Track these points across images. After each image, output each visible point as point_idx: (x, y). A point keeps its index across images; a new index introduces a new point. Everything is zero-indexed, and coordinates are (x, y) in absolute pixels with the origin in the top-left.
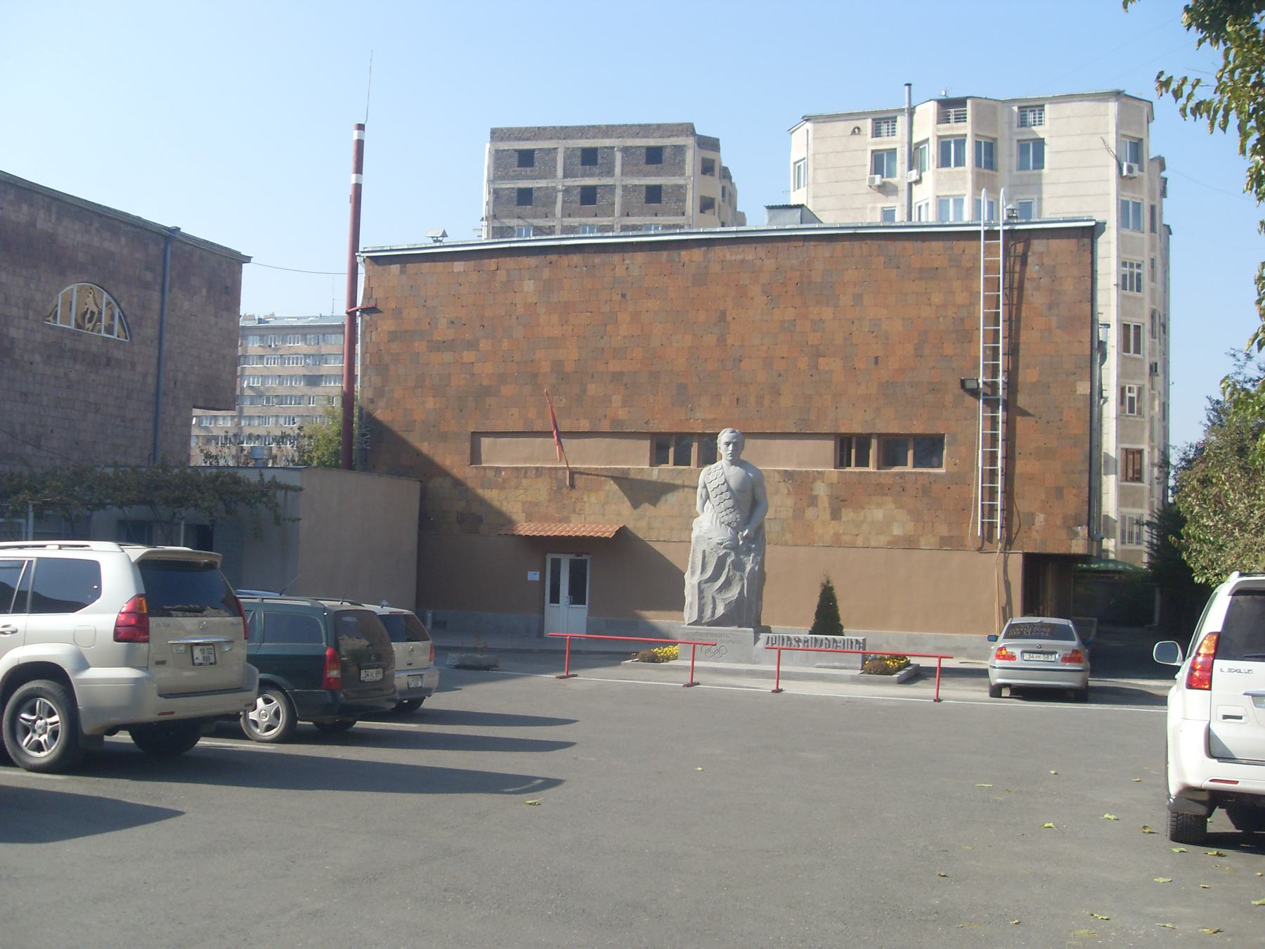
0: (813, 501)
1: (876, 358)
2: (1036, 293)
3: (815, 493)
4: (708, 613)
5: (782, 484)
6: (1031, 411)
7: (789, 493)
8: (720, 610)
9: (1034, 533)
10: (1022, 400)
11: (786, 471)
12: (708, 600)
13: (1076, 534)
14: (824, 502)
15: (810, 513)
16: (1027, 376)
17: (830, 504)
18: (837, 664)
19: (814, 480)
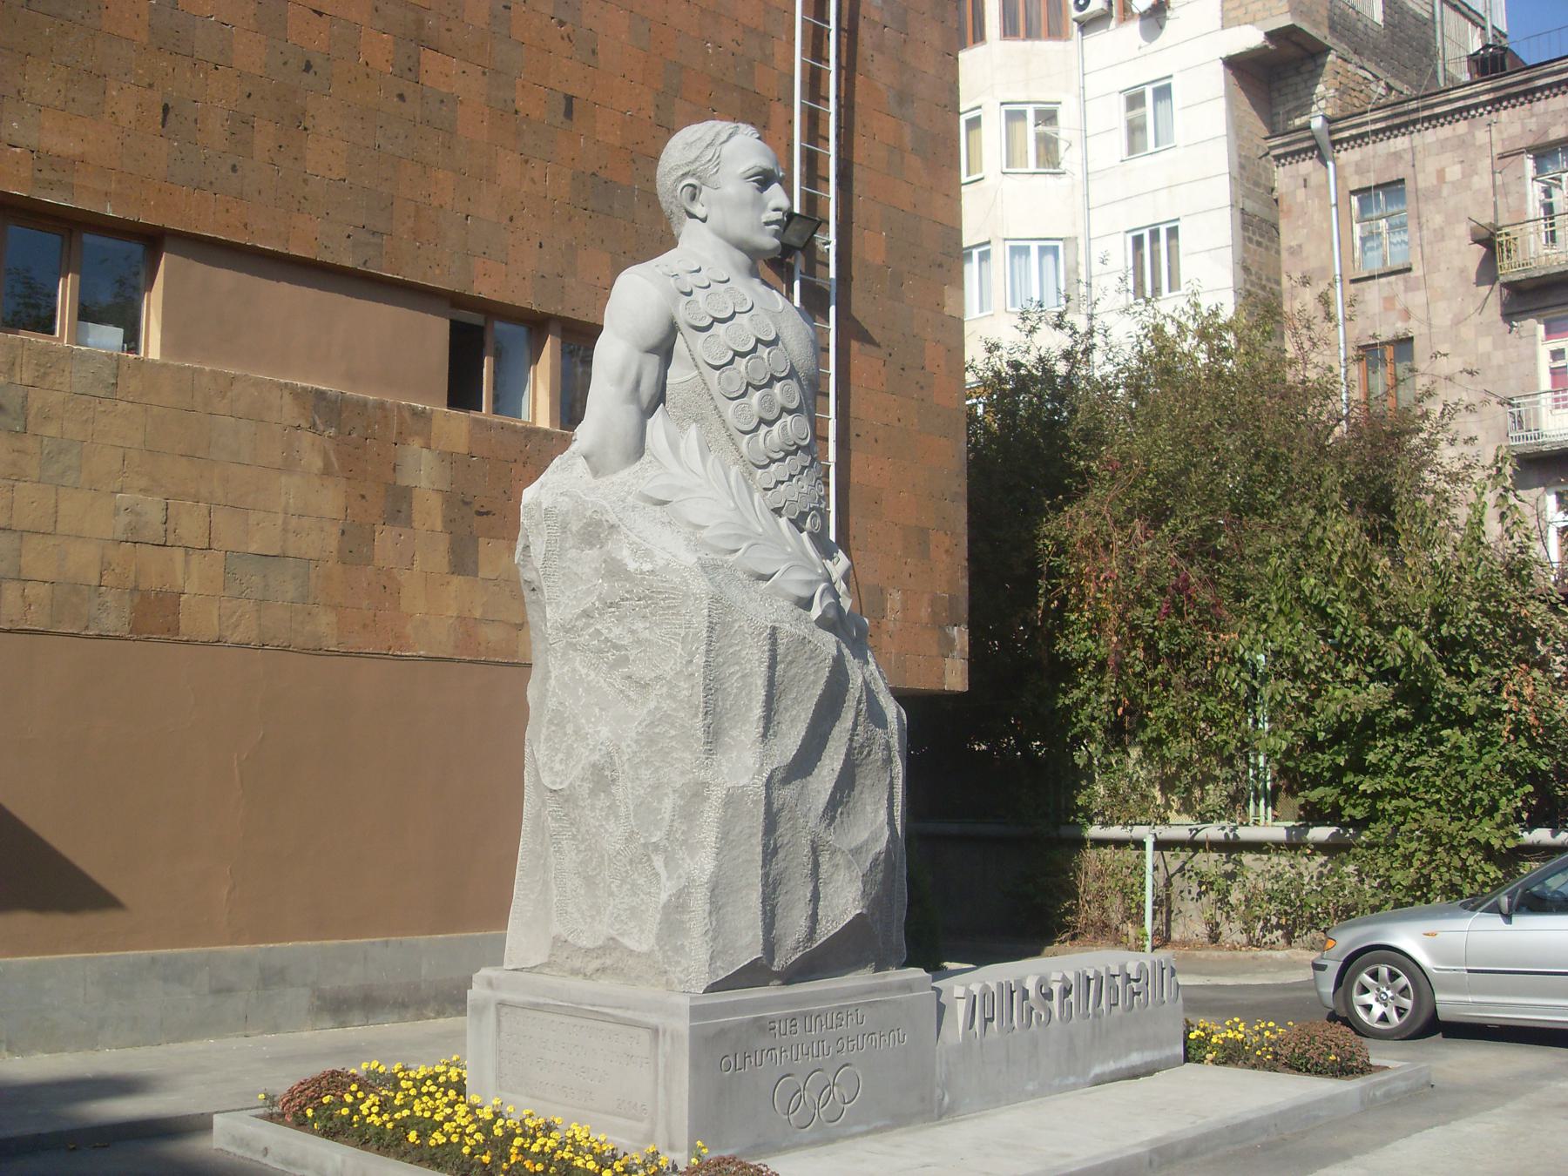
0: (398, 505)
1: (569, 100)
2: (877, 57)
3: (404, 481)
4: (793, 927)
5: (307, 438)
6: (876, 334)
7: (327, 472)
8: (845, 902)
9: (885, 637)
10: (861, 307)
11: (320, 395)
12: (796, 859)
13: (950, 642)
14: (429, 510)
15: (386, 540)
16: (870, 247)
17: (449, 522)
18: (1135, 1059)
19: (402, 439)
